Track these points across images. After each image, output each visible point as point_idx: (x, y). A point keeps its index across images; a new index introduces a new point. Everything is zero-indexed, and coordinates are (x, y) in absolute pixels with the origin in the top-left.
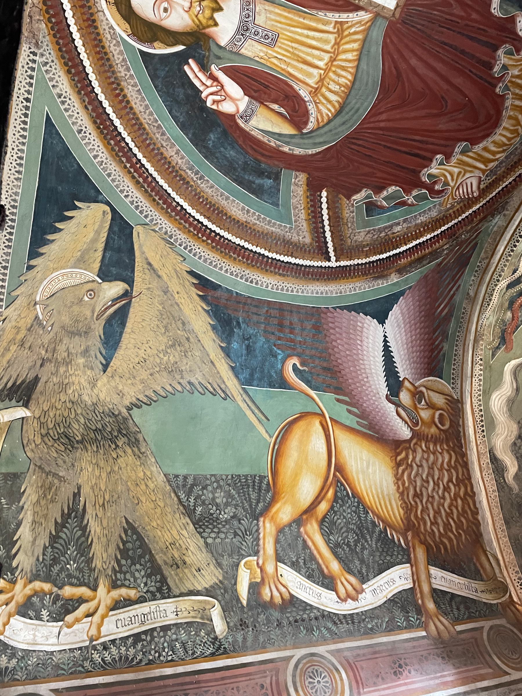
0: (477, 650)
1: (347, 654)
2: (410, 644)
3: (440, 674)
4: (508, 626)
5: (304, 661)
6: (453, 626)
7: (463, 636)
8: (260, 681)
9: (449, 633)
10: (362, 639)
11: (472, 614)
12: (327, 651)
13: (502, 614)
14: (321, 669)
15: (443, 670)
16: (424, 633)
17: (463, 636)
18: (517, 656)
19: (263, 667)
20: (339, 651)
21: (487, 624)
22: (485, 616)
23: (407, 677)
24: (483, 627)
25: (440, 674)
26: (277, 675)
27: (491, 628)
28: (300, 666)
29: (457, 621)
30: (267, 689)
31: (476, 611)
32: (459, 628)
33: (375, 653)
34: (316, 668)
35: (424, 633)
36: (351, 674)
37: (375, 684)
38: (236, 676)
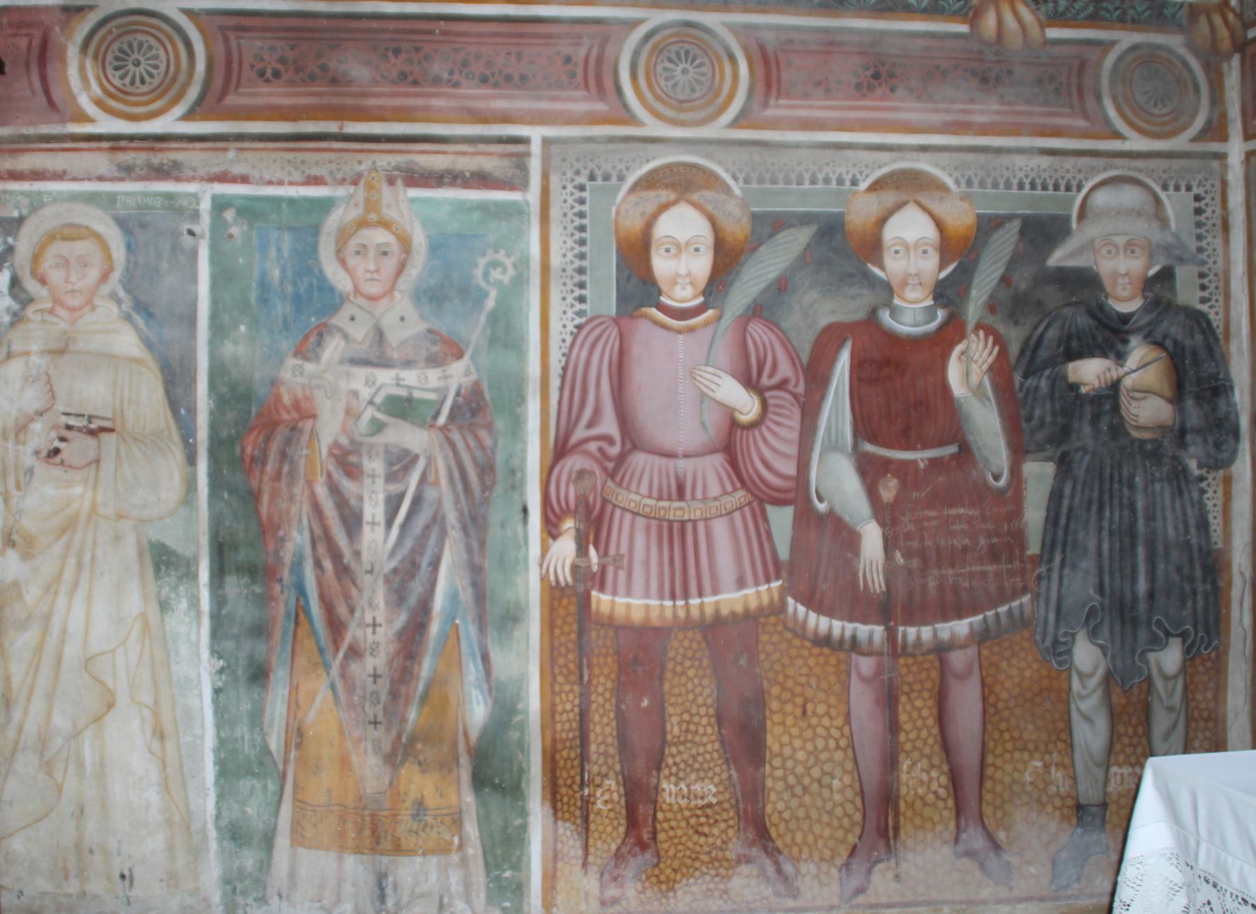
0: (1074, 80)
1: (770, 38)
2: (921, 43)
3: (961, 106)
4: (1182, 51)
5: (667, 32)
6: (1042, 27)
7: (1057, 50)
8: (565, 49)
9: (1025, 36)
10: (810, 14)
11: (1103, 13)
12: (725, 25)
13: (1180, 25)
14: (697, 51)
15: (972, 101)
16: (964, 28)
17: (1057, 50)
18: (1165, 111)
19: (578, 29)
20: (748, 27)
21: (1127, 38)
22: (1133, 21)
23: (882, 98)
24: (1113, 43)
25: (961, 106)
26: (602, 47)
27: (1135, 48)
28: (657, 38)
29: (1058, 19)
30: (575, 65)
31: (1117, 9)
32: (1054, 33)
33: (831, 43)
34: (687, 46)
35: (964, 28)
36: (760, 70)
37: (806, 96)
38: (521, 35)
